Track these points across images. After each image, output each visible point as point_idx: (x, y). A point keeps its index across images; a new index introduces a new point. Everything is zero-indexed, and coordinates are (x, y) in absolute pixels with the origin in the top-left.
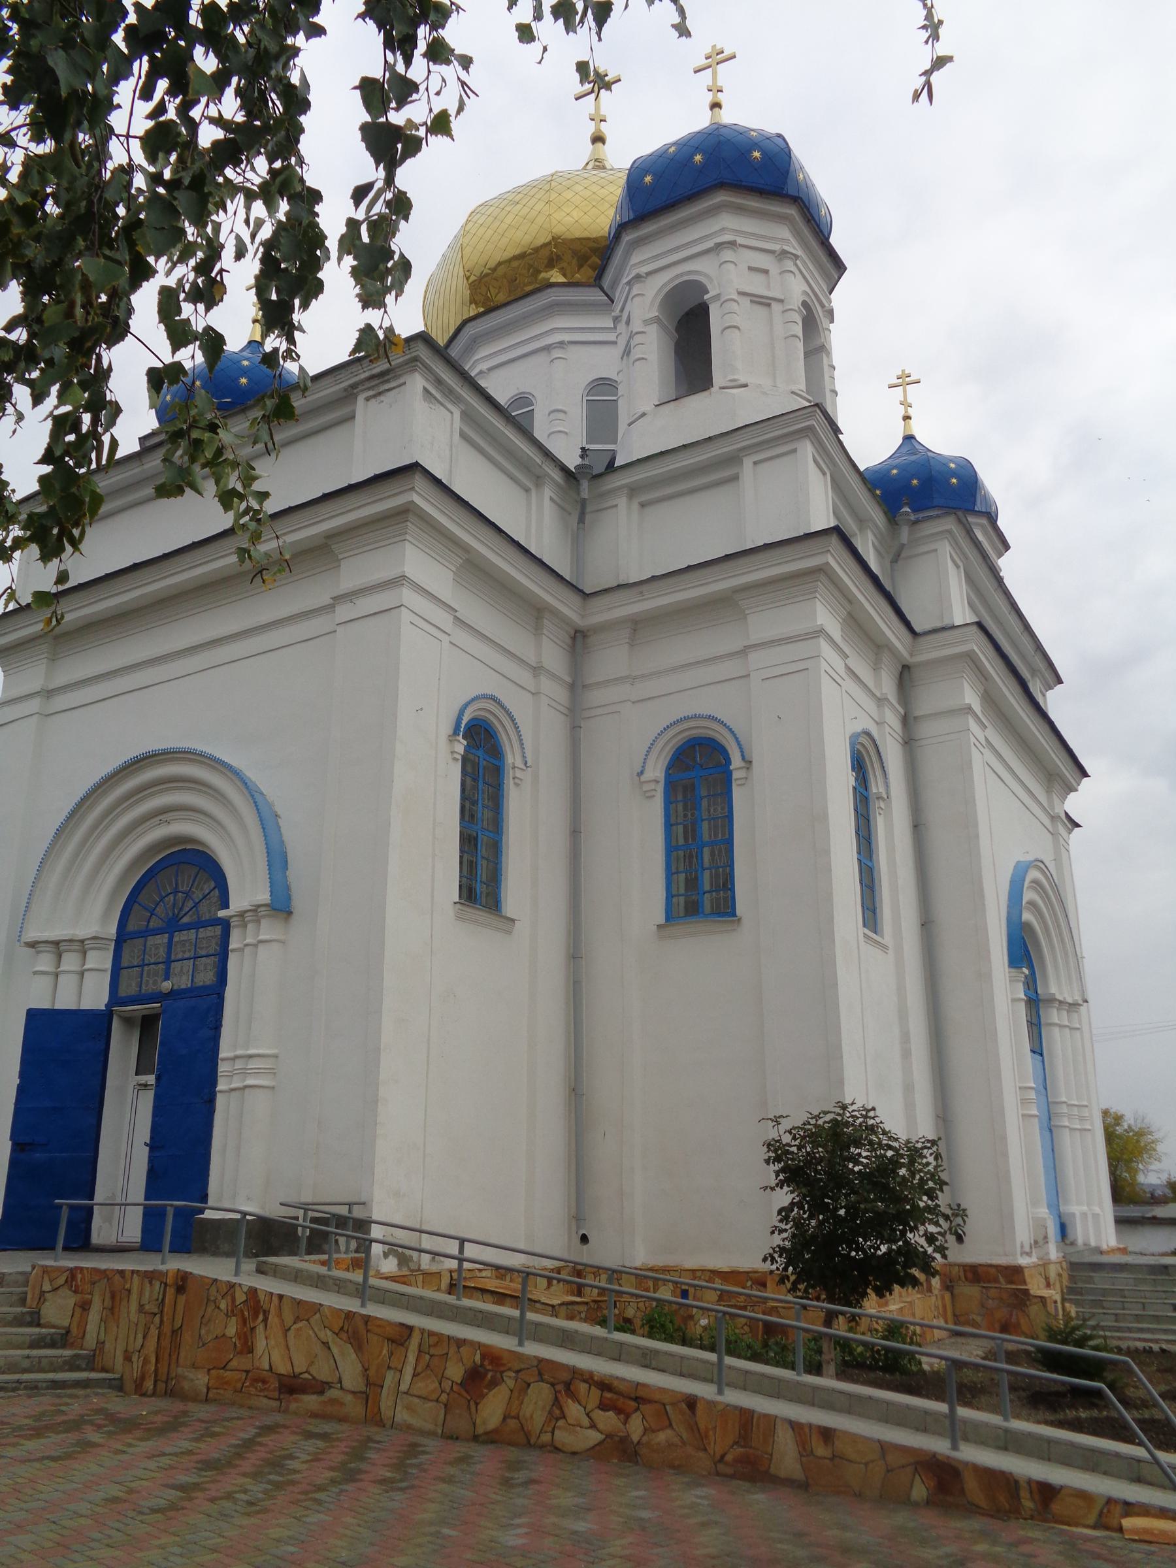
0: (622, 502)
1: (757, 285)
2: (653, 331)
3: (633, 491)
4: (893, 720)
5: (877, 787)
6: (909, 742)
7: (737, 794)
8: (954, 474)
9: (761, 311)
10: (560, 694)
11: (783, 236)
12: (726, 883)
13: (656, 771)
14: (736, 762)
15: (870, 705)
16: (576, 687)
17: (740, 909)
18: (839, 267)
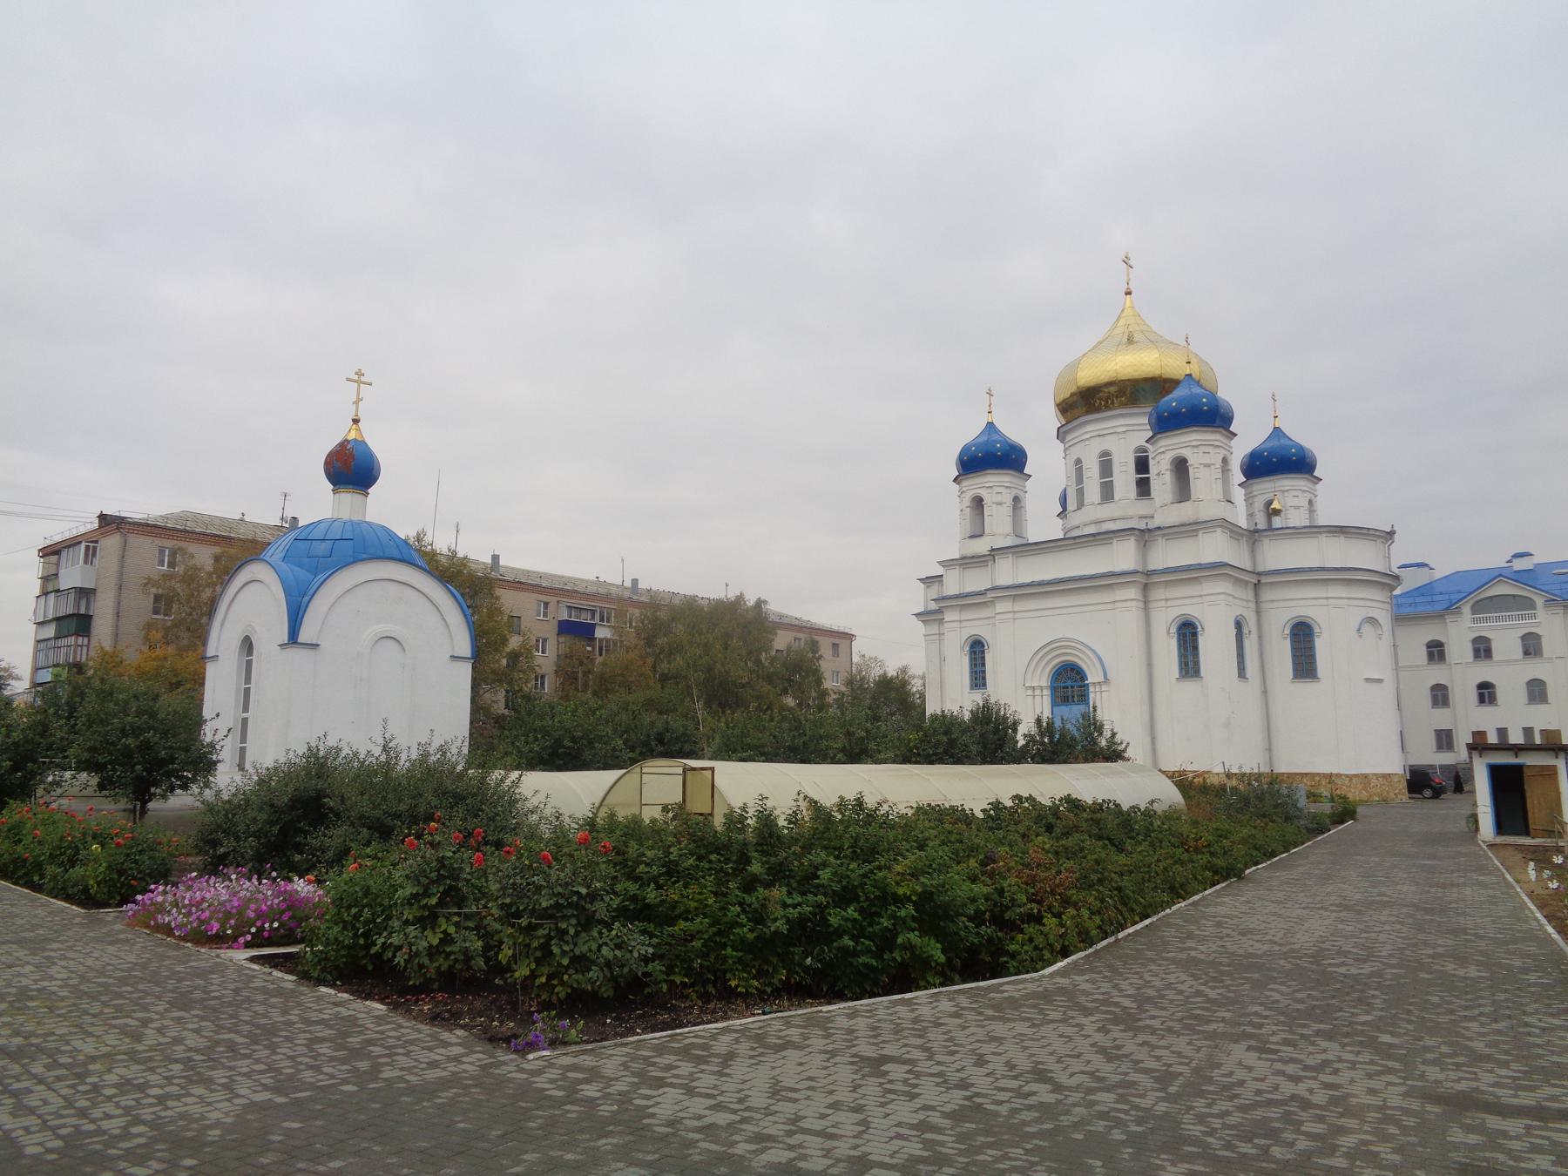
0: (1160, 538)
1: (1207, 461)
2: (1168, 473)
3: (1164, 535)
4: (1252, 605)
5: (1245, 631)
6: (1258, 612)
7: (1201, 640)
8: (1294, 455)
9: (1207, 469)
10: (1142, 605)
11: (1214, 437)
12: (1197, 664)
13: (1174, 630)
14: (1199, 629)
15: (1244, 604)
16: (1146, 602)
17: (1203, 673)
18: (1236, 435)
